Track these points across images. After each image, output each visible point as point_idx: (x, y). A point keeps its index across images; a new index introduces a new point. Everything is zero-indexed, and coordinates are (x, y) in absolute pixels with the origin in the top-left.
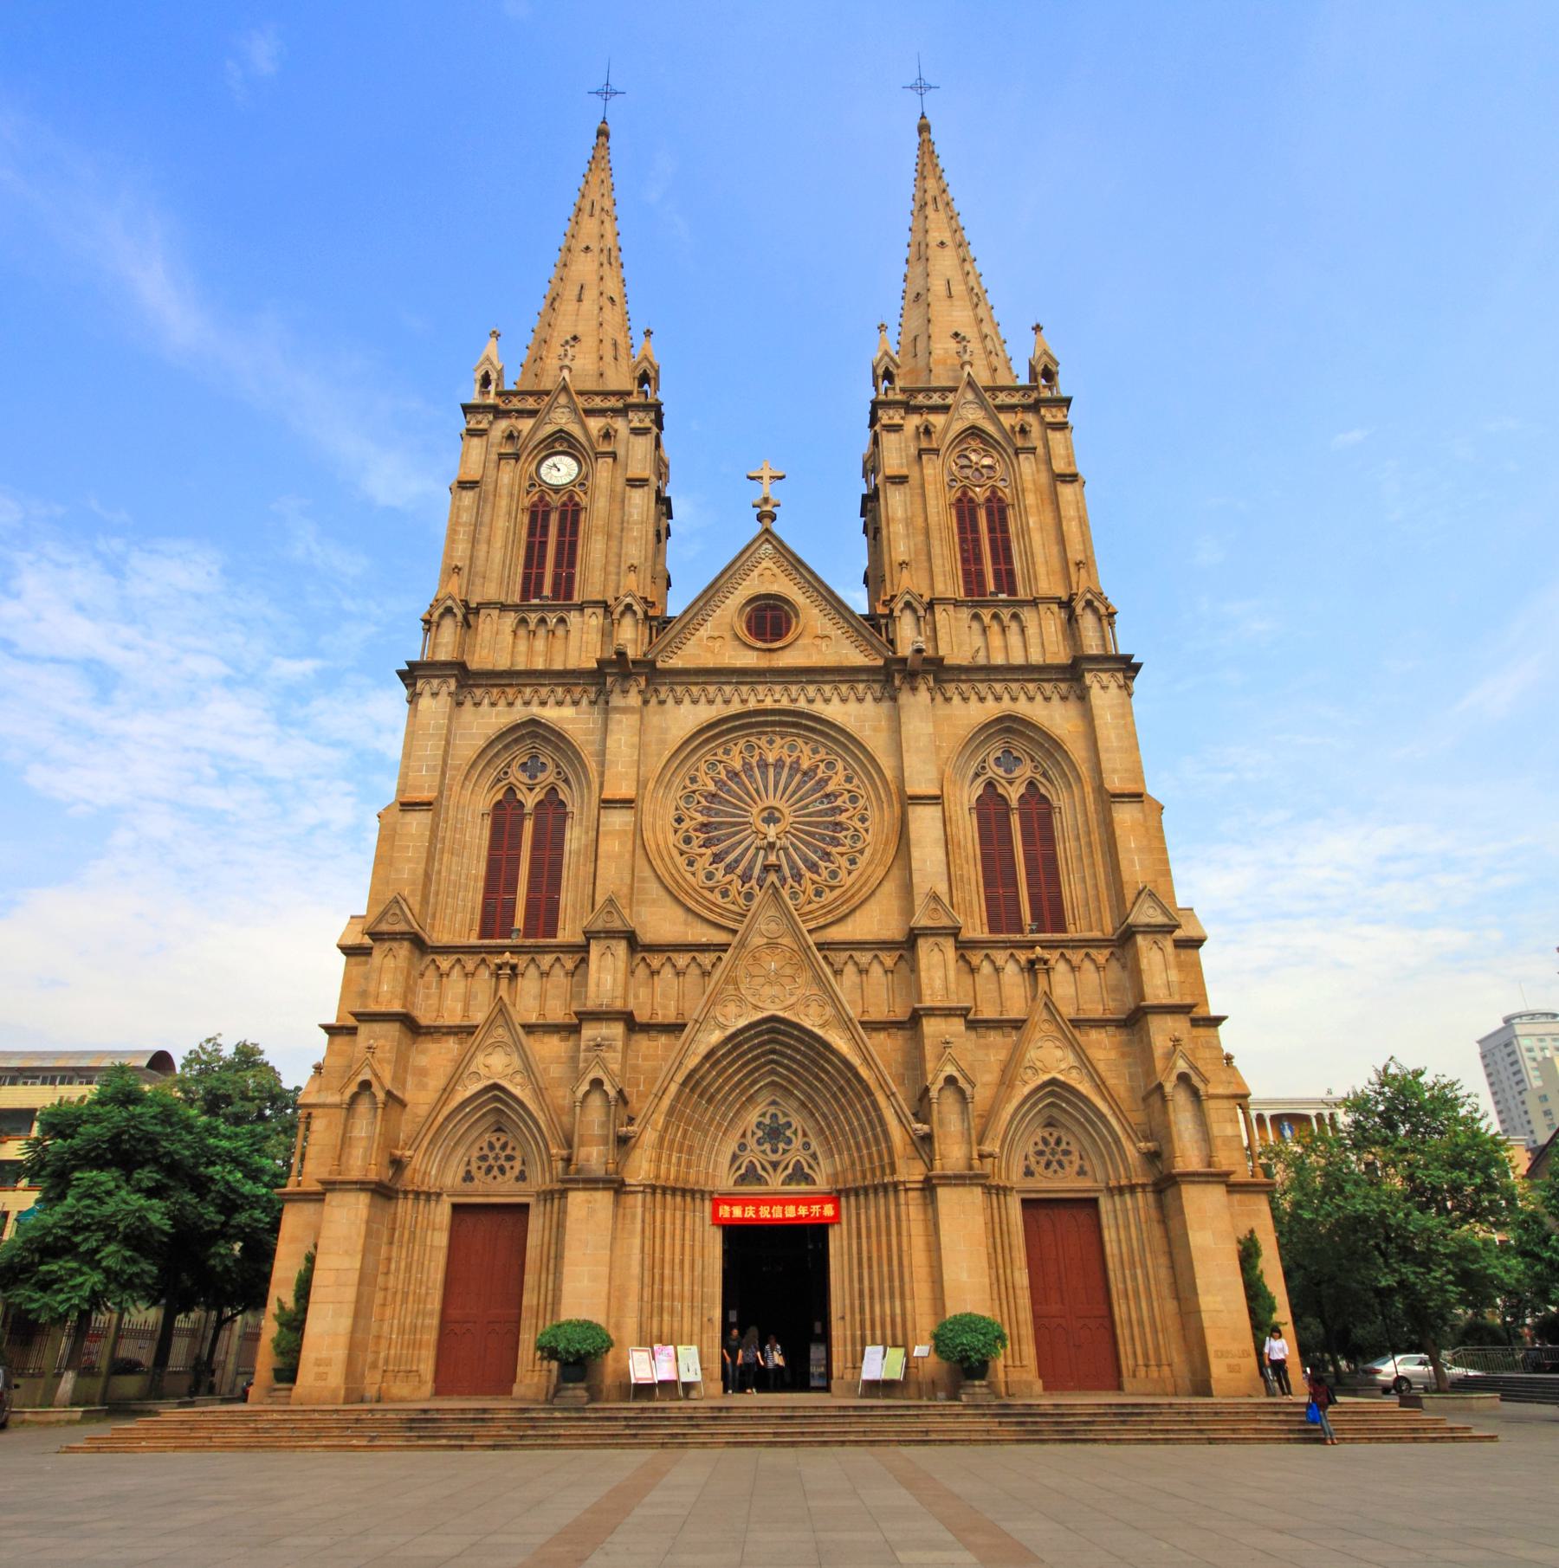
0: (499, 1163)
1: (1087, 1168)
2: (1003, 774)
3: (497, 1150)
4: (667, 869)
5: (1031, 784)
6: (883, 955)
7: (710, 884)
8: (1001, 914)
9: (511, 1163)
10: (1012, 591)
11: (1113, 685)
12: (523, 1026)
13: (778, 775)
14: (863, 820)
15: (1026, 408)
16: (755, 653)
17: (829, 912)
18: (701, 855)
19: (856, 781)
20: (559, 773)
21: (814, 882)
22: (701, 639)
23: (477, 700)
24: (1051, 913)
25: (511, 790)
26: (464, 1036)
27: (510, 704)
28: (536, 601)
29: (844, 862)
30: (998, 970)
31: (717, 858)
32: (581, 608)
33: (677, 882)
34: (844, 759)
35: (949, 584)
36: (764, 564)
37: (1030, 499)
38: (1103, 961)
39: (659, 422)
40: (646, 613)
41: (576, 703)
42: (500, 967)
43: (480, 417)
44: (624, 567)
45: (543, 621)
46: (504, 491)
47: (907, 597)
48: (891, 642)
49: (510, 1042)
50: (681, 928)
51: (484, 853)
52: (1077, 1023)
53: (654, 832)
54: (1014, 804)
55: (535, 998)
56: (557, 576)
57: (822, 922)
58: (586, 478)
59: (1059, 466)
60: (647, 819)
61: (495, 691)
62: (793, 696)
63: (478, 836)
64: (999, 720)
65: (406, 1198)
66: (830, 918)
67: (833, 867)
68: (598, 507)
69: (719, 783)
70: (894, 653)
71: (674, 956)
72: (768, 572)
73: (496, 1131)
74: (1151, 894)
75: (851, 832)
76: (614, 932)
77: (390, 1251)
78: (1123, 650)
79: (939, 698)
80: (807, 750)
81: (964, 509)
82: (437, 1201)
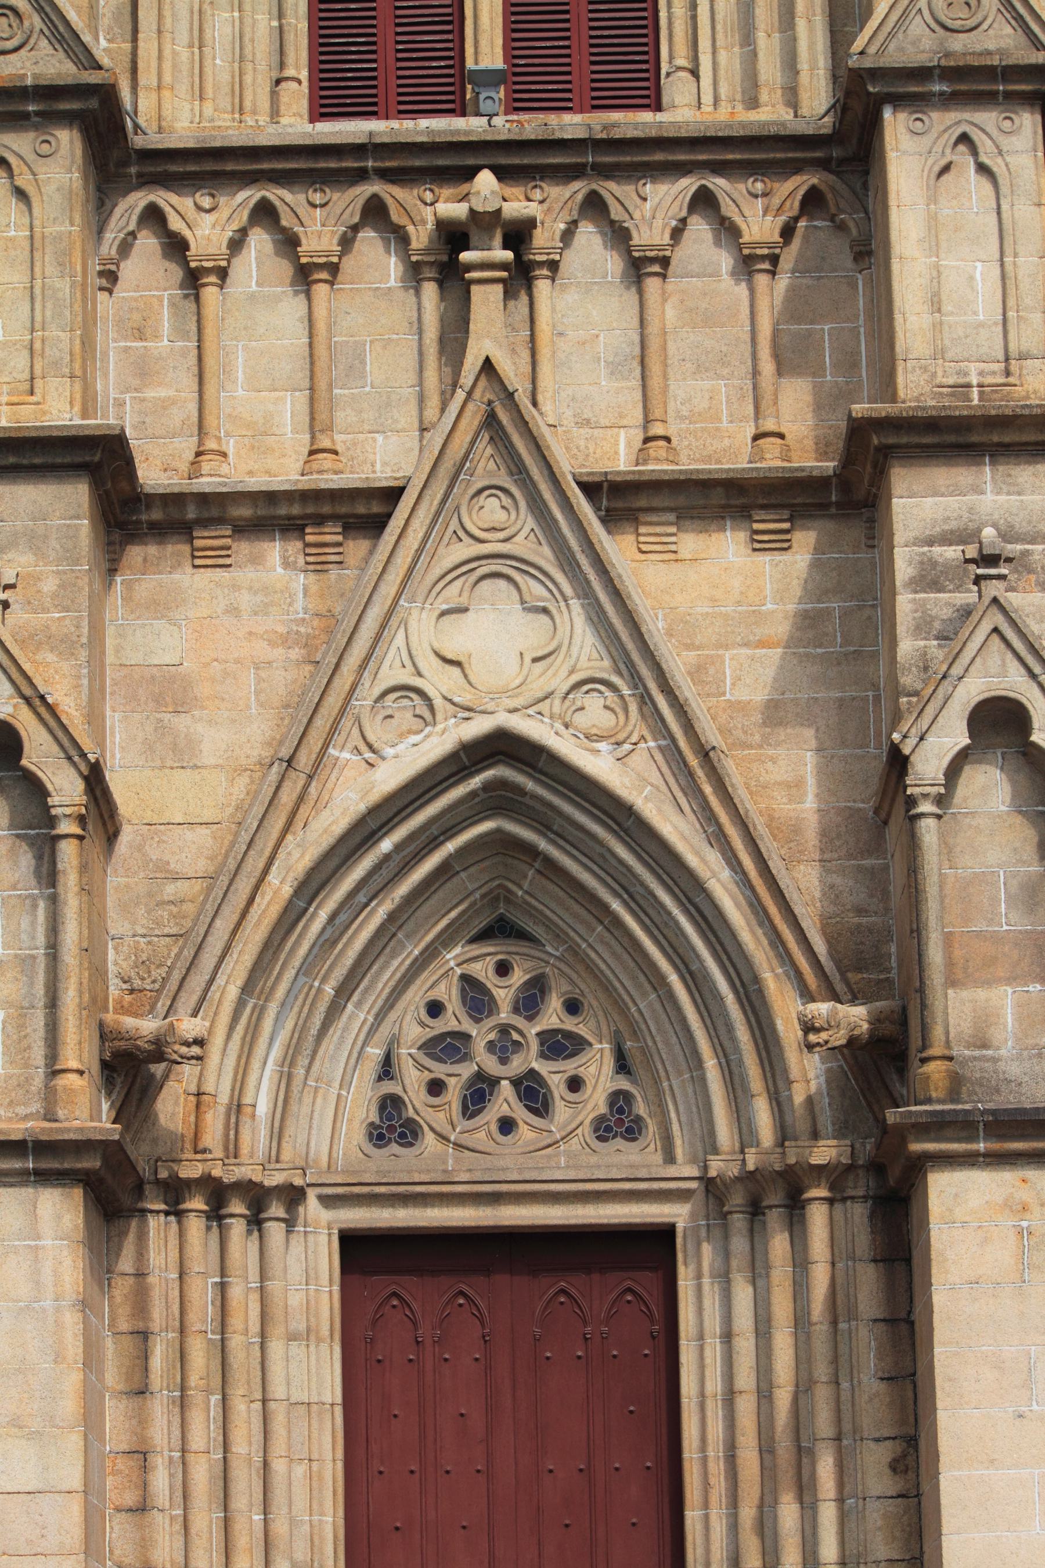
0: (517, 1065)
3: (505, 1015)
9: (570, 1067)
12: (590, 489)
26: (331, 533)
49: (545, 556)
55: (615, 370)
65: (178, 1213)
73: (482, 936)
76: (989, 73)
77: (142, 1420)
82: (290, 1223)
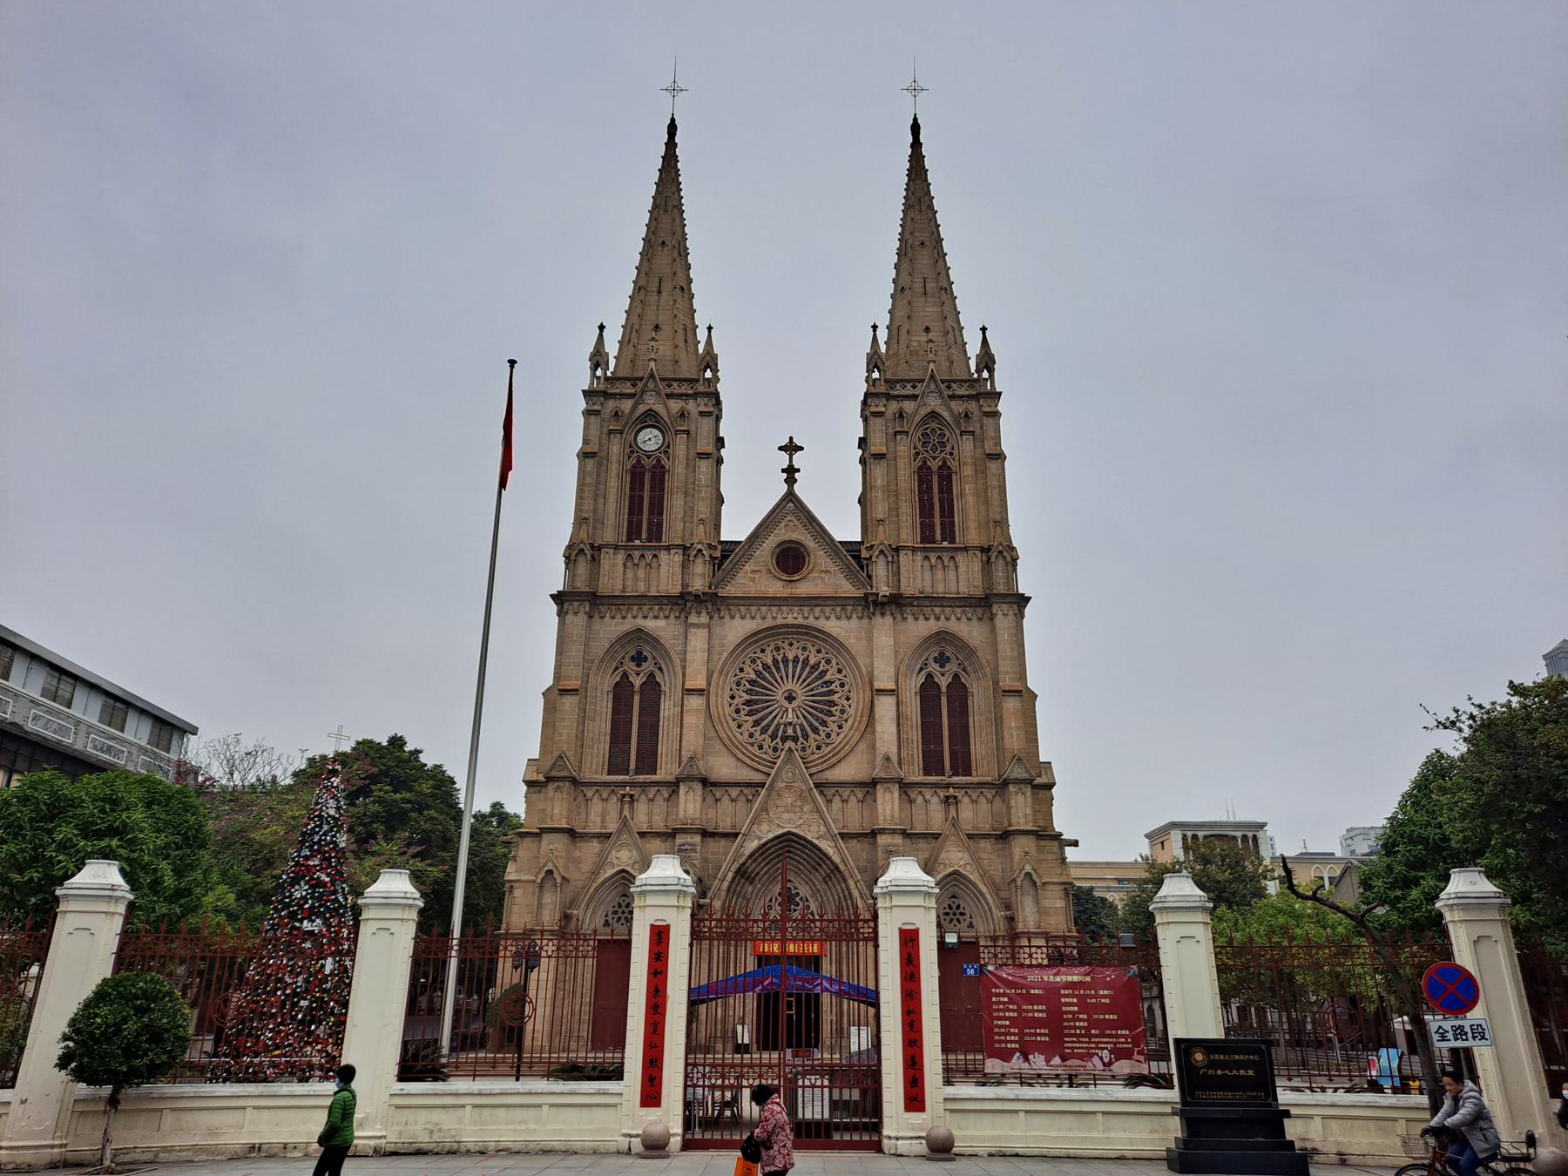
1: (974, 921)
2: (938, 668)
4: (725, 732)
5: (956, 676)
6: (857, 791)
7: (751, 740)
8: (932, 763)
10: (953, 541)
11: (1011, 613)
13: (795, 667)
14: (848, 699)
15: (970, 397)
16: (782, 583)
17: (825, 761)
18: (746, 721)
19: (844, 672)
20: (655, 664)
21: (816, 741)
22: (746, 573)
23: (602, 615)
24: (963, 764)
25: (625, 675)
27: (624, 618)
28: (637, 542)
29: (834, 727)
30: (927, 801)
31: (756, 723)
32: (668, 548)
33: (730, 739)
34: (836, 657)
35: (908, 534)
36: (789, 518)
37: (968, 471)
38: (990, 796)
39: (718, 403)
40: (711, 556)
41: (666, 618)
42: (624, 796)
43: (595, 399)
44: (695, 520)
45: (643, 556)
46: (614, 459)
47: (882, 547)
48: (870, 577)
50: (734, 771)
51: (609, 717)
52: (970, 836)
53: (717, 705)
54: (944, 689)
56: (650, 522)
57: (820, 768)
58: (668, 447)
59: (989, 447)
60: (713, 698)
61: (614, 607)
62: (806, 615)
63: (603, 707)
64: (937, 634)
66: (825, 765)
67: (828, 730)
68: (678, 471)
69: (758, 673)
70: (872, 587)
71: (729, 789)
72: (792, 524)
74: (1019, 759)
75: (839, 708)
78: (1020, 592)
79: (899, 617)
80: (813, 650)
81: (923, 474)
